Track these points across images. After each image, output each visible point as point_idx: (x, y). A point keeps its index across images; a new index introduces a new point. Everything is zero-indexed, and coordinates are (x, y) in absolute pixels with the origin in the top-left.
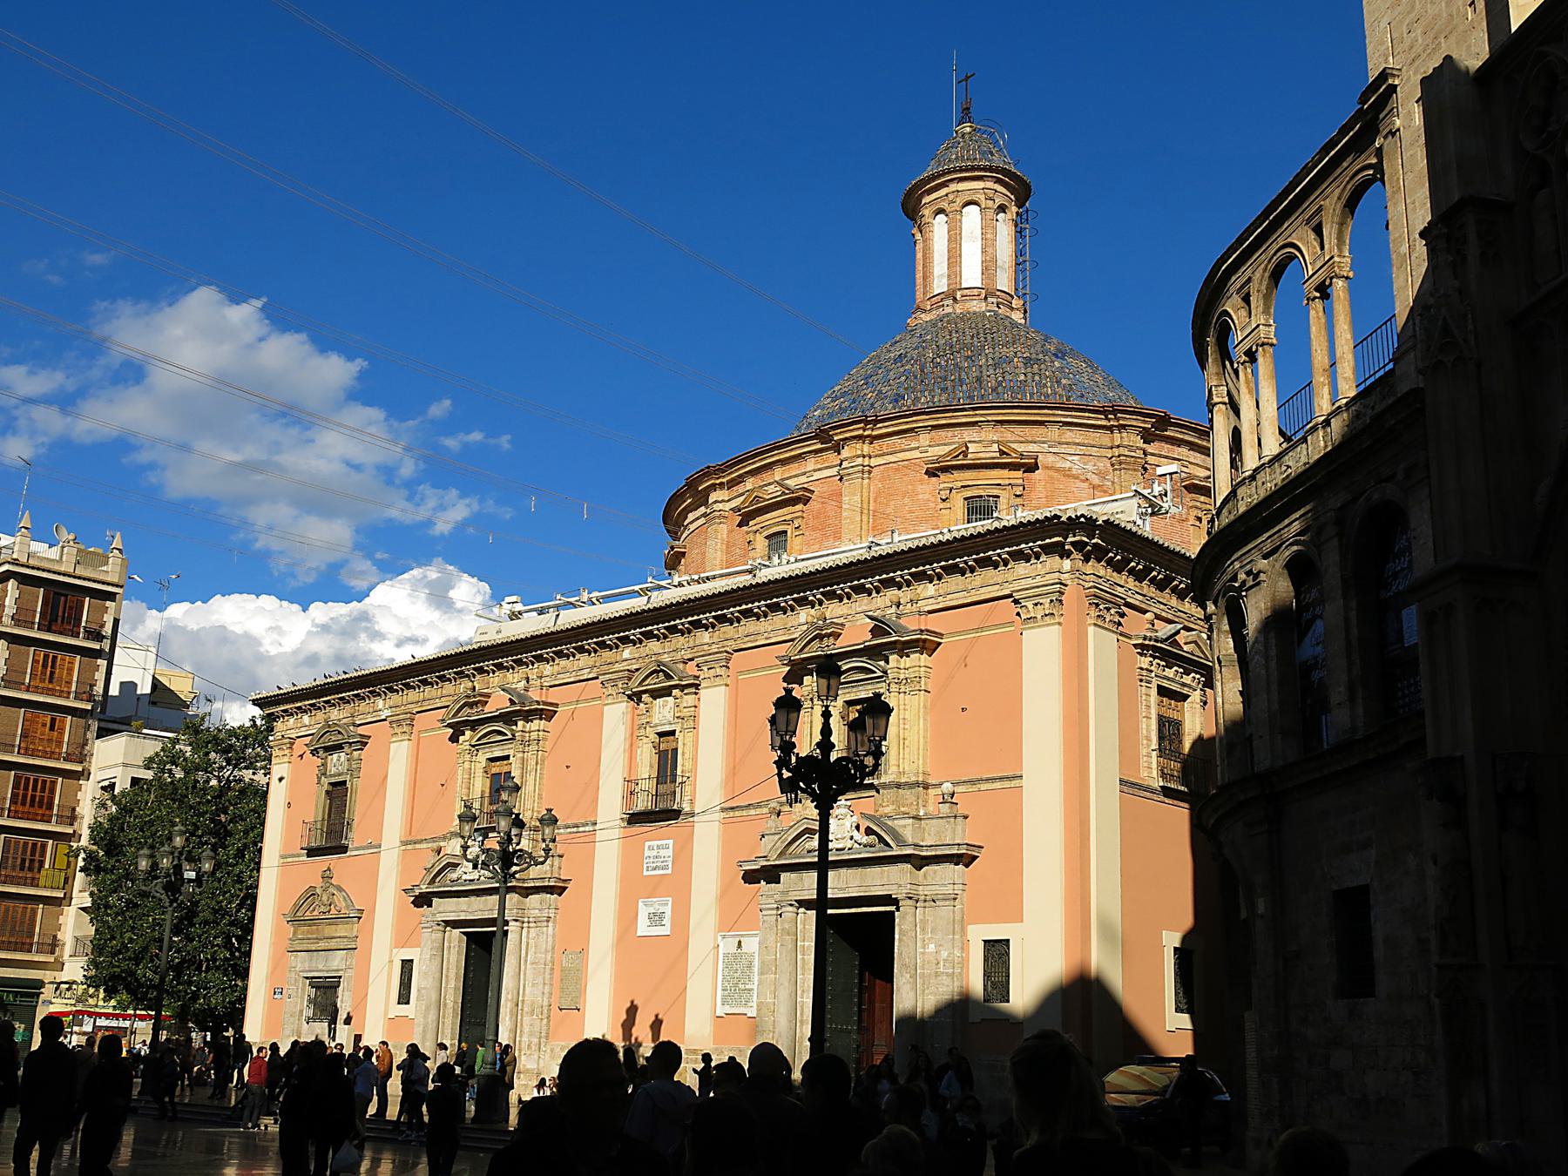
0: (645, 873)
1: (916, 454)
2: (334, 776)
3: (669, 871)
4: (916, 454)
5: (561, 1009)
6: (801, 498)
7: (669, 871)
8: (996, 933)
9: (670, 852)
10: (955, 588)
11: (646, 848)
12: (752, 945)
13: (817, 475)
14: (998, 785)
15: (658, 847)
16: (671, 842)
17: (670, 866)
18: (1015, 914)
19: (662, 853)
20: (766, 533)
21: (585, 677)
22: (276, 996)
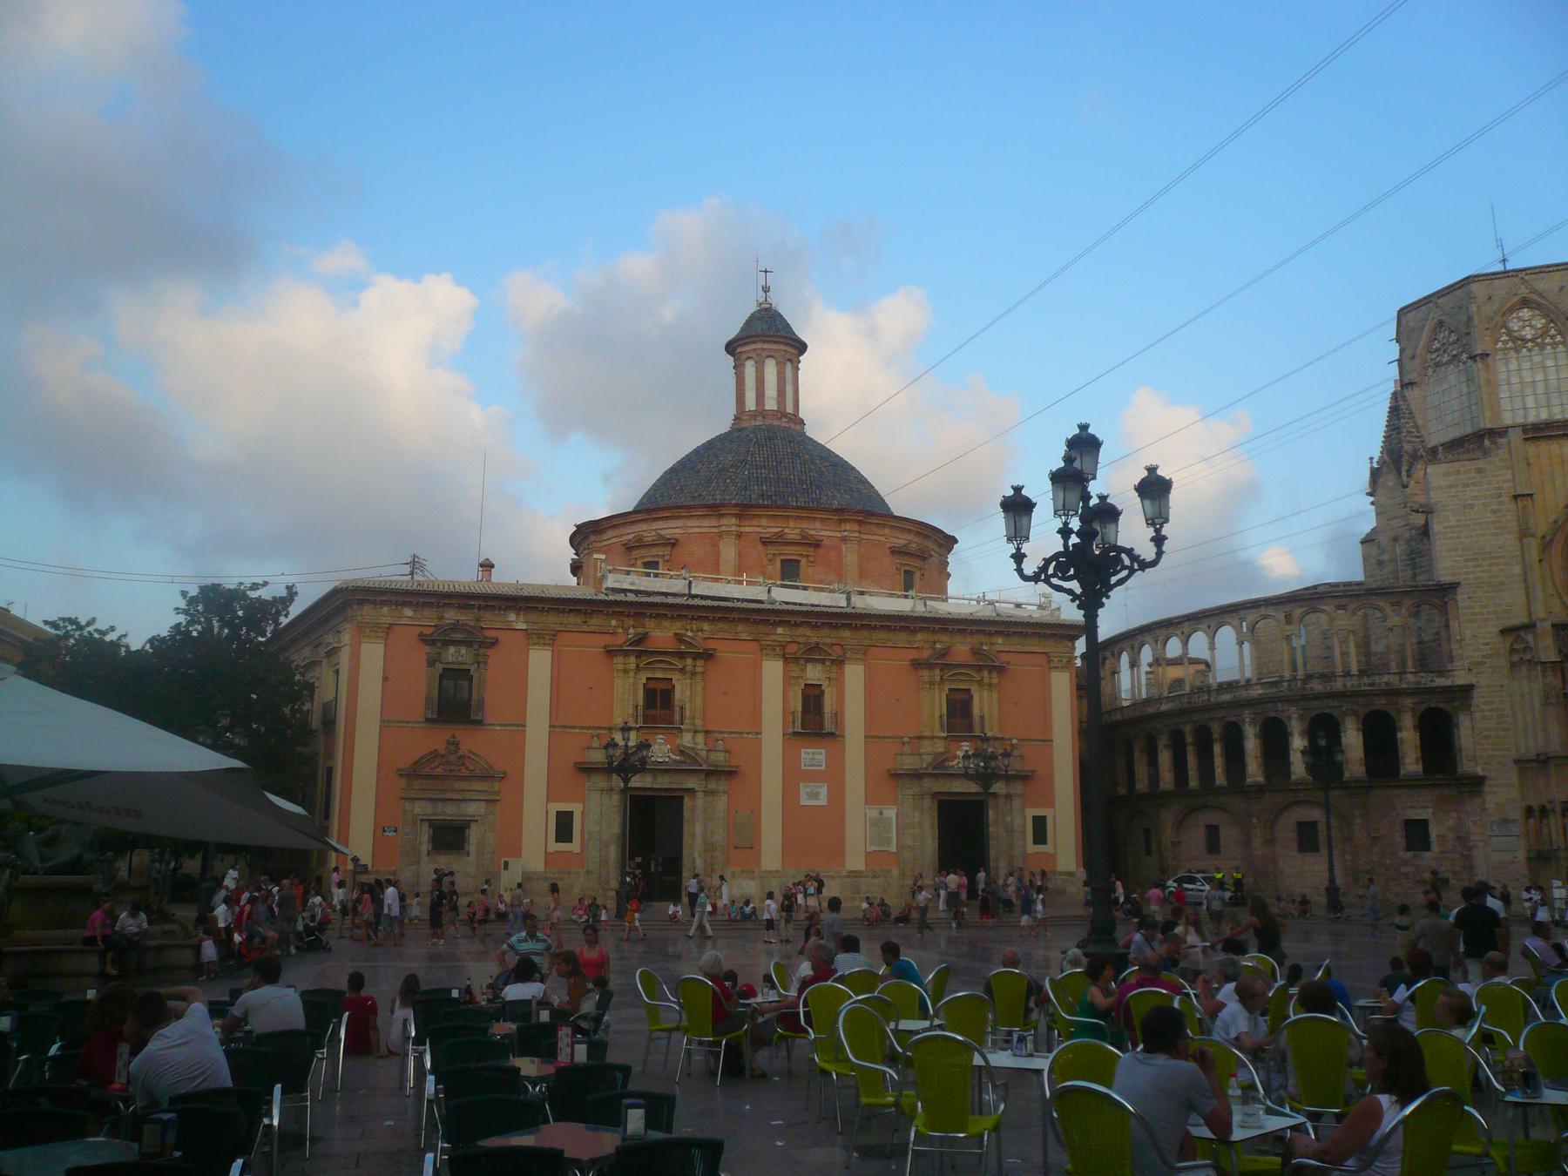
0: (803, 768)
1: (883, 539)
2: (453, 663)
3: (823, 768)
4: (883, 539)
5: (736, 848)
6: (817, 545)
7: (823, 768)
8: (1040, 812)
9: (823, 757)
10: (1016, 645)
11: (803, 753)
12: (891, 813)
13: (823, 533)
14: (1038, 743)
15: (813, 753)
16: (823, 751)
17: (824, 765)
18: (1051, 804)
19: (817, 757)
20: (783, 558)
21: (743, 638)
22: (387, 834)
